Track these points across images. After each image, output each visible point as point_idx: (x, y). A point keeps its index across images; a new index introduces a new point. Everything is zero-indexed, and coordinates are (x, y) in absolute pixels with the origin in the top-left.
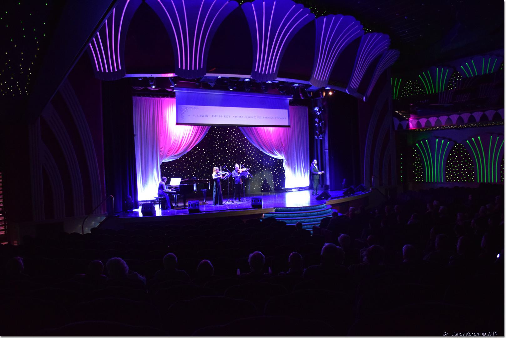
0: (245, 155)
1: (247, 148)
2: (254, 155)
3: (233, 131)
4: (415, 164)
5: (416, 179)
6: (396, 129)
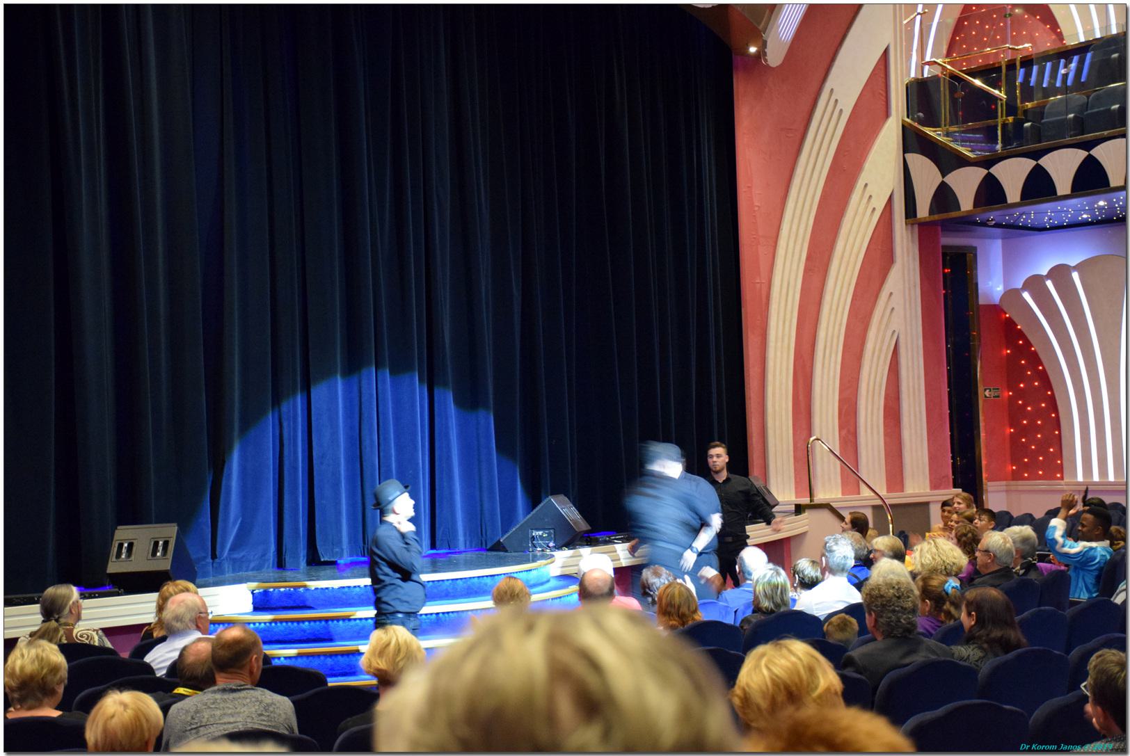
6: (923, 211)
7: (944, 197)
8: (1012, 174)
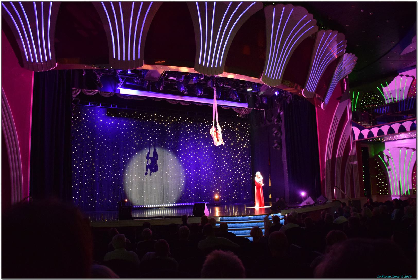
0: (200, 165)
1: (203, 158)
2: (210, 165)
3: (188, 140)
4: (379, 176)
5: (380, 192)
6: (357, 138)
7: (361, 136)
8: (375, 131)
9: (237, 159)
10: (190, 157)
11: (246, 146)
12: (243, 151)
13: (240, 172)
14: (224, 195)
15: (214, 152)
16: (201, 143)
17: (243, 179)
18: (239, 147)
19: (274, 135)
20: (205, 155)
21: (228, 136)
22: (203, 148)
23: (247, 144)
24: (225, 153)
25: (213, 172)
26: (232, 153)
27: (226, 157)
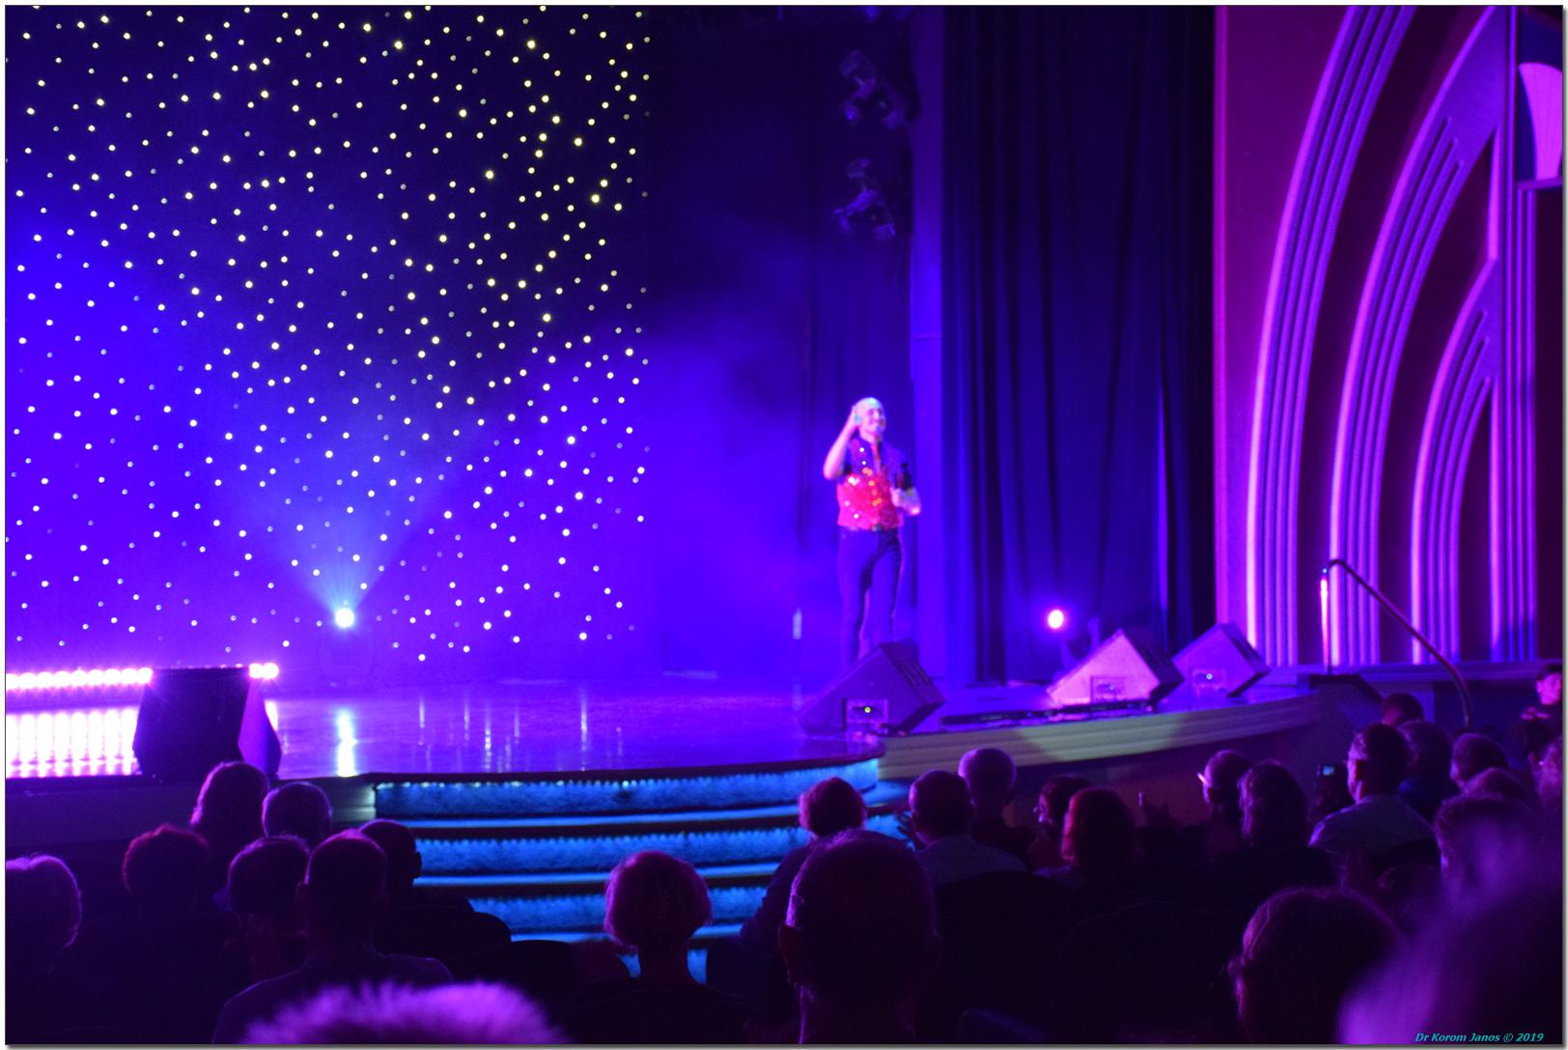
1: (230, 282)
2: (296, 350)
9: (523, 308)
10: (108, 264)
11: (609, 196)
12: (584, 241)
13: (555, 416)
14: (407, 610)
15: (334, 239)
16: (211, 149)
17: (571, 480)
18: (553, 203)
19: (852, 114)
20: (244, 254)
21: (453, 101)
22: (231, 193)
23: (615, 178)
24: (425, 249)
25: (317, 410)
26: (483, 249)
27: (437, 280)
